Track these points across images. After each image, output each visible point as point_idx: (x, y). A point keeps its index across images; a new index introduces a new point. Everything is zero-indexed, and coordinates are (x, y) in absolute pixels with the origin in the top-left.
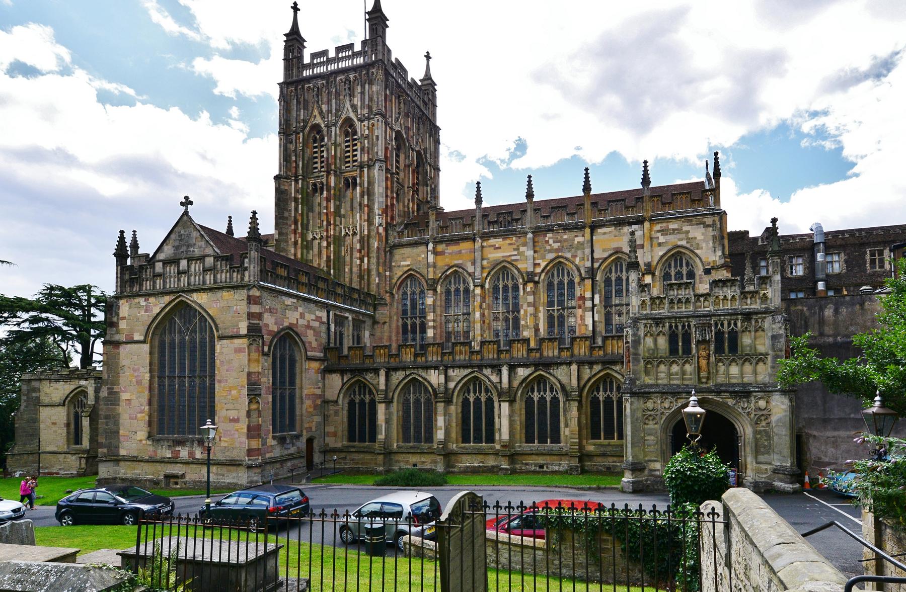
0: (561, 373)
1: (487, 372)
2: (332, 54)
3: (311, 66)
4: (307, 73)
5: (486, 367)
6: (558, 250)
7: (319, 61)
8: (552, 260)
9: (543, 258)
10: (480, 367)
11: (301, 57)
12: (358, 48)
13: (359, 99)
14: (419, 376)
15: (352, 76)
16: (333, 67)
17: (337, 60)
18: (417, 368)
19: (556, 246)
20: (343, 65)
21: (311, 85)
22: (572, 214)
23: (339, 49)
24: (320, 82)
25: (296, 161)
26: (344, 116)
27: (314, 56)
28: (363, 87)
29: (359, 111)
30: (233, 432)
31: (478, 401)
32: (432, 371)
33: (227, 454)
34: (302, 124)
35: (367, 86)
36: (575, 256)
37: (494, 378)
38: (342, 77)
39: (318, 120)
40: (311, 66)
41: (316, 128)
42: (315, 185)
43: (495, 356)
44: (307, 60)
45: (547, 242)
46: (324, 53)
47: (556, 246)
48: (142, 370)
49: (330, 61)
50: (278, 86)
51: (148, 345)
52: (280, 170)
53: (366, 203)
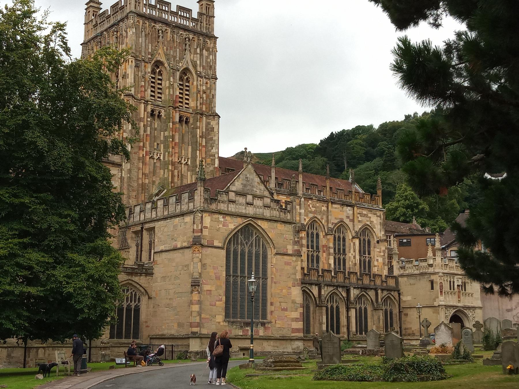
0: (372, 293)
1: (340, 289)
2: (174, 9)
5: (340, 286)
6: (314, 213)
8: (311, 218)
9: (307, 216)
10: (337, 286)
13: (199, 58)
14: (308, 289)
15: (191, 37)
18: (306, 283)
19: (313, 209)
21: (158, 26)
22: (320, 191)
23: (180, 8)
24: (164, 28)
25: (144, 86)
26: (185, 66)
28: (201, 50)
29: (199, 69)
30: (283, 318)
31: (332, 307)
32: (314, 286)
33: (280, 332)
34: (150, 56)
35: (204, 51)
36: (322, 219)
37: (344, 295)
38: (184, 33)
39: (163, 59)
41: (158, 64)
42: (153, 111)
43: (342, 281)
45: (309, 205)
47: (313, 209)
48: (220, 268)
51: (225, 250)
53: (204, 144)
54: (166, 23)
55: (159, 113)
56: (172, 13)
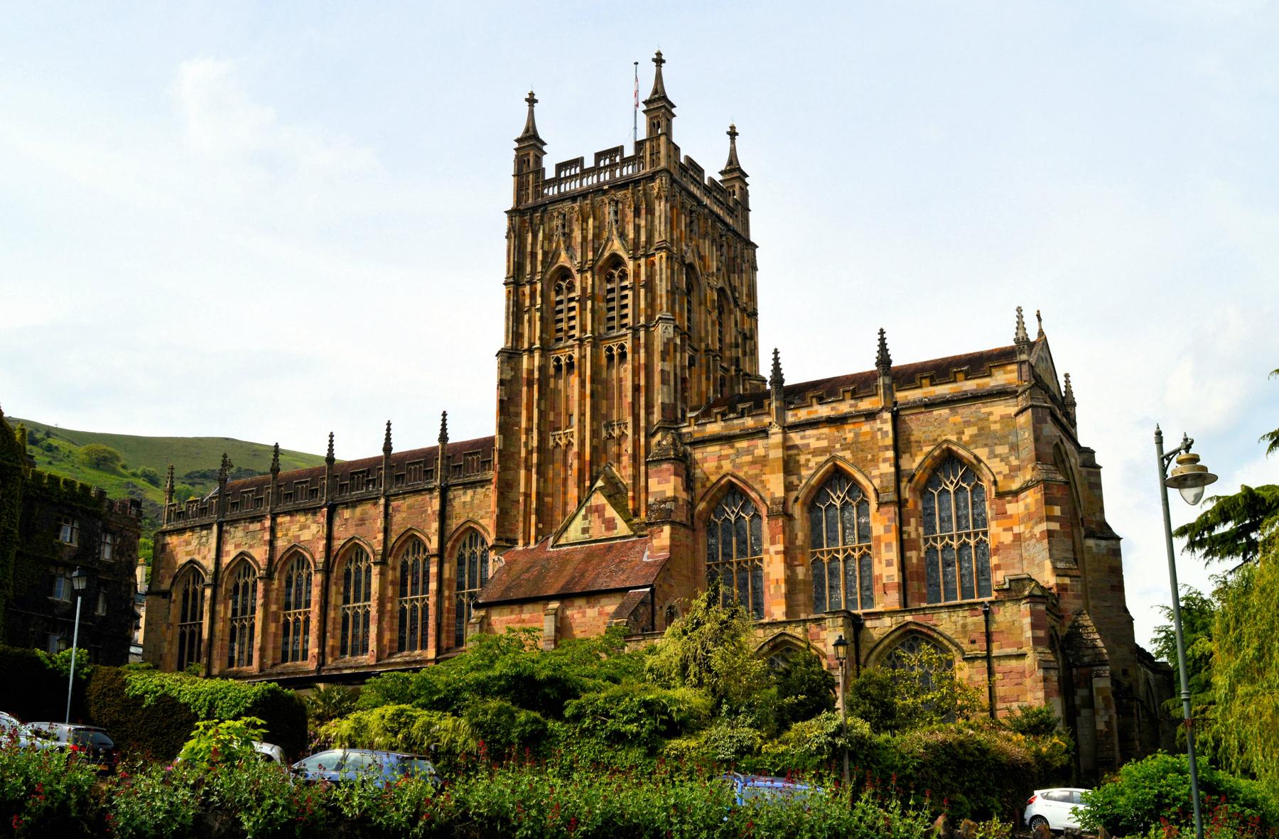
3: (557, 181)
4: (552, 191)
7: (568, 174)
11: (540, 171)
12: (629, 152)
16: (591, 181)
17: (596, 170)
20: (605, 177)
23: (599, 156)
27: (560, 167)
40: (557, 181)
44: (550, 173)
46: (578, 162)
49: (586, 173)
50: (506, 215)
52: (507, 343)
54: (573, 197)
55: (570, 357)
56: (596, 170)
